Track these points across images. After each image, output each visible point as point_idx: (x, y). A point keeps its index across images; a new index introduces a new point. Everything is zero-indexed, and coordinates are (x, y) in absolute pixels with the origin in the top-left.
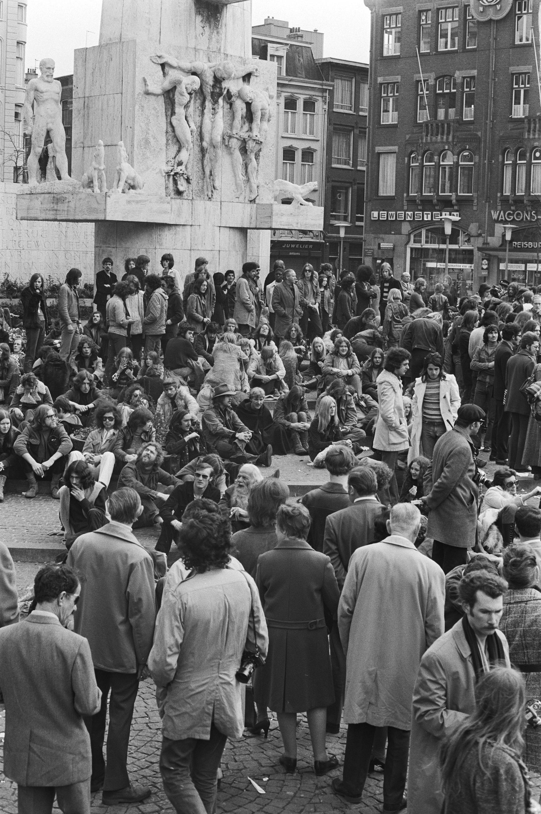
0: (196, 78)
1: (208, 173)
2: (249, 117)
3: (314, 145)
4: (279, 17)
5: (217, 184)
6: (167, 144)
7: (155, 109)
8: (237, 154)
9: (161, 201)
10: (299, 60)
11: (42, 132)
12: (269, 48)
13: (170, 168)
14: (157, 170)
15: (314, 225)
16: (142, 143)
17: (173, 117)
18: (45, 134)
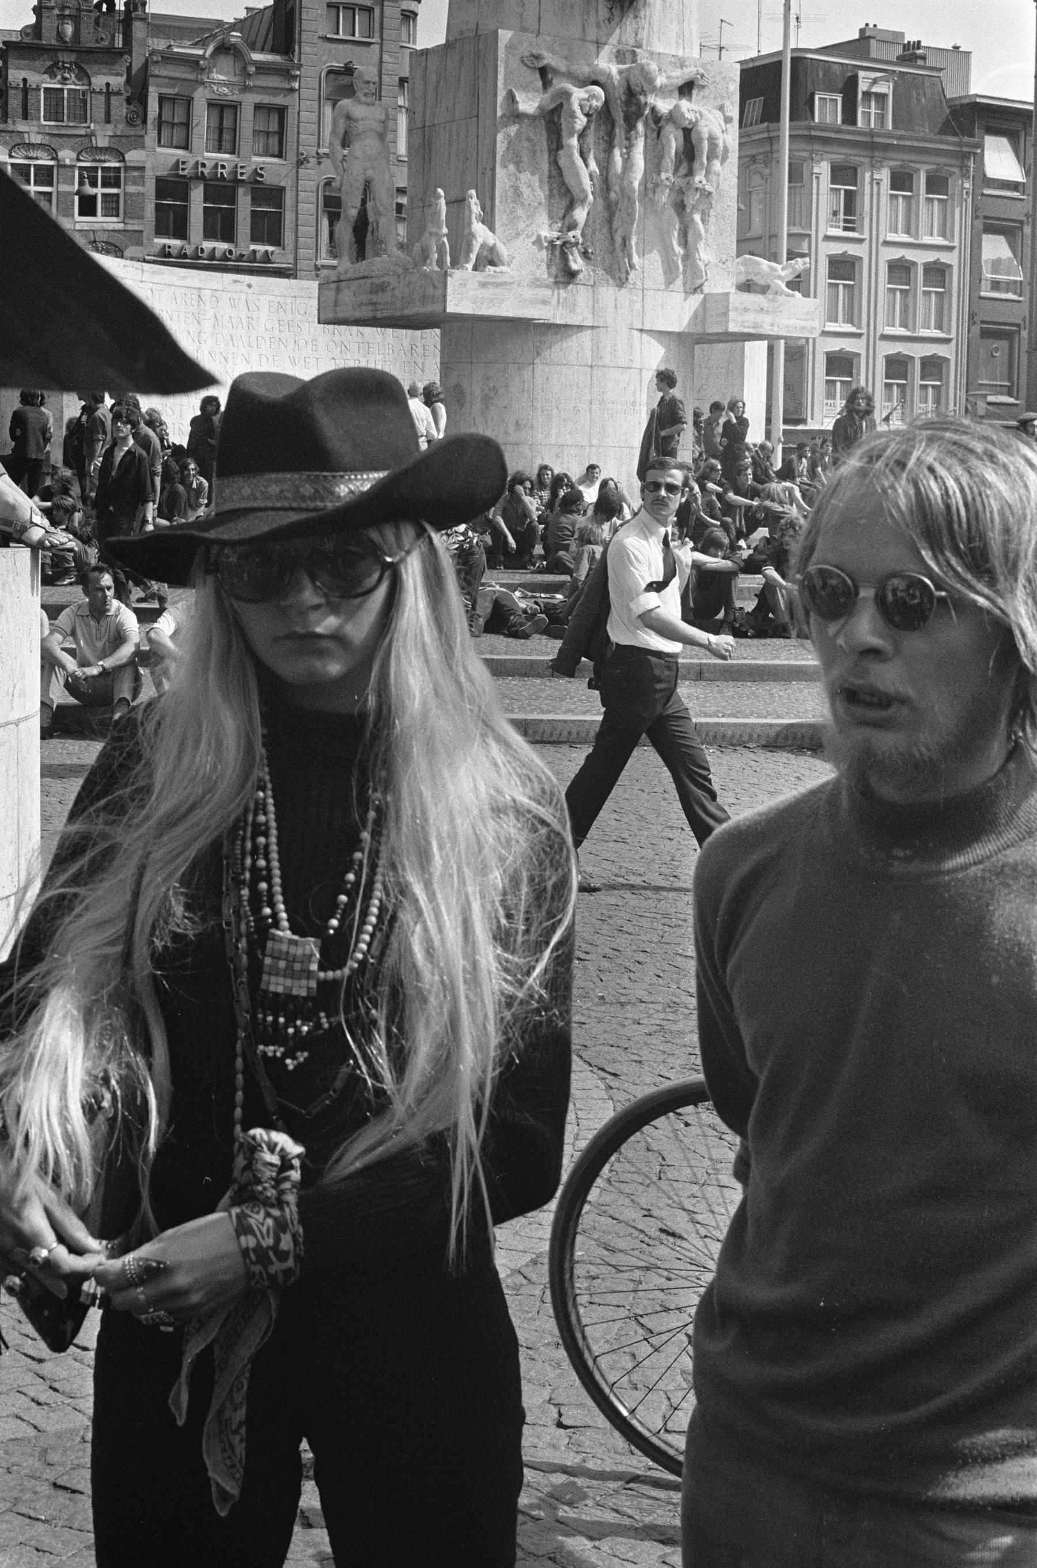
0: (598, 90)
1: (618, 240)
2: (689, 153)
3: (945, 258)
4: (887, 24)
9: (536, 283)
10: (918, 100)
11: (357, 184)
12: (860, 80)
13: (556, 234)
14: (534, 238)
15: (802, 328)
16: (509, 194)
17: (561, 152)
18: (362, 187)
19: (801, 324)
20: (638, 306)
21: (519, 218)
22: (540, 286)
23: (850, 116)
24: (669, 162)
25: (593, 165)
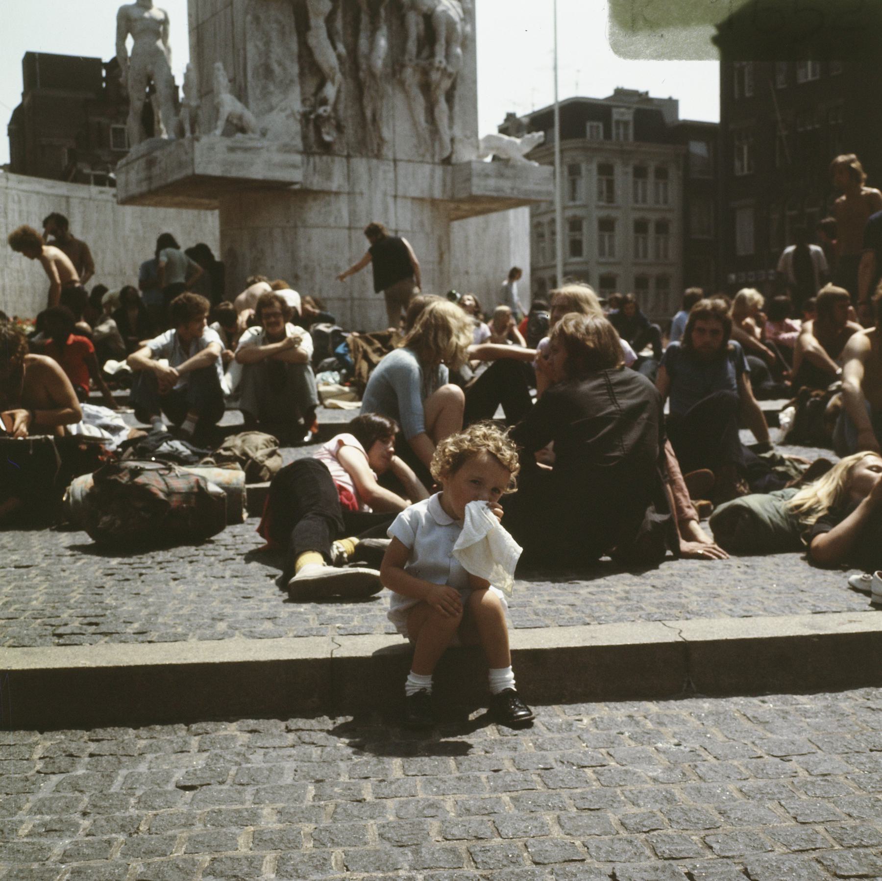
5: (386, 133)
6: (302, 75)
7: (278, 22)
8: (415, 92)
9: (286, 149)
19: (537, 188)
20: (391, 175)
21: (271, 93)
22: (288, 152)
23: (608, 135)
24: (412, 46)
25: (341, 48)
